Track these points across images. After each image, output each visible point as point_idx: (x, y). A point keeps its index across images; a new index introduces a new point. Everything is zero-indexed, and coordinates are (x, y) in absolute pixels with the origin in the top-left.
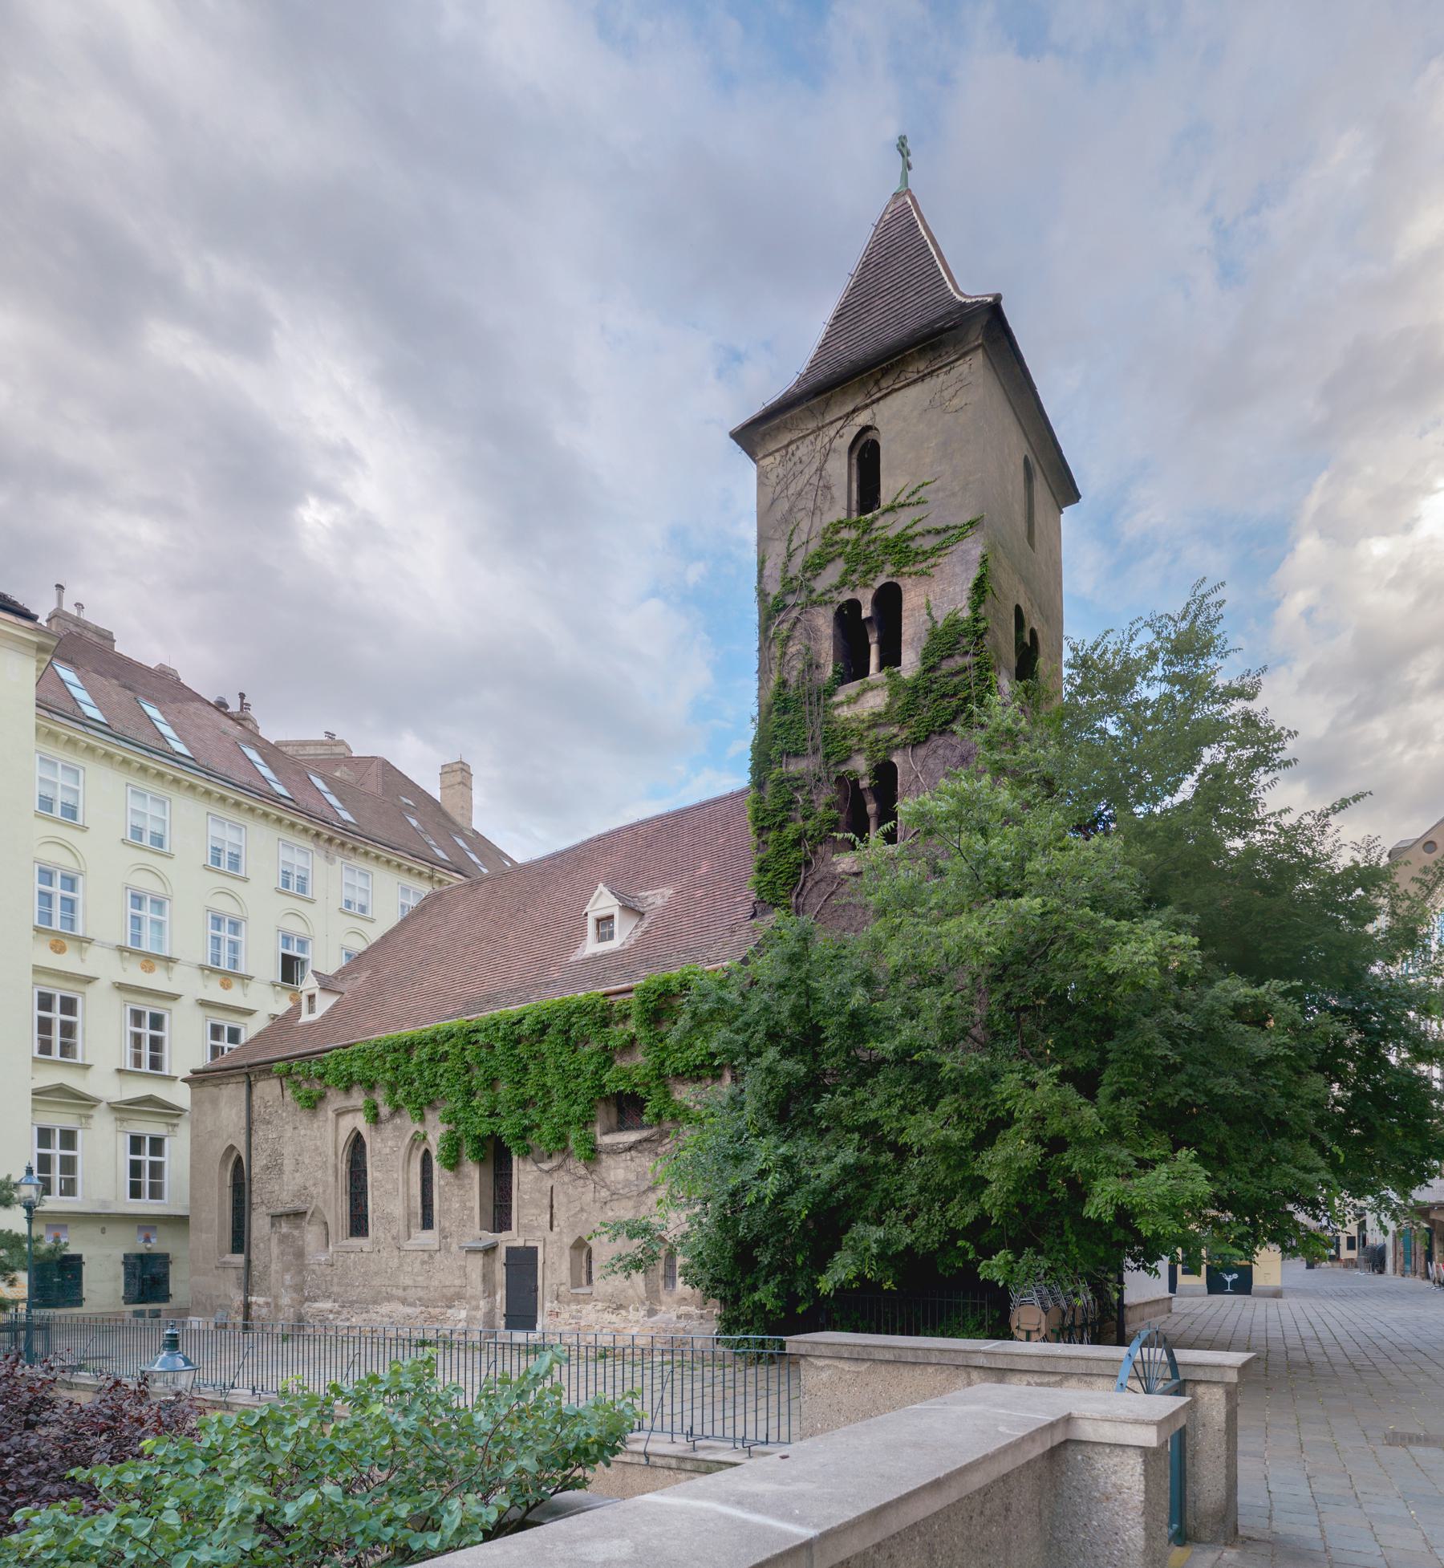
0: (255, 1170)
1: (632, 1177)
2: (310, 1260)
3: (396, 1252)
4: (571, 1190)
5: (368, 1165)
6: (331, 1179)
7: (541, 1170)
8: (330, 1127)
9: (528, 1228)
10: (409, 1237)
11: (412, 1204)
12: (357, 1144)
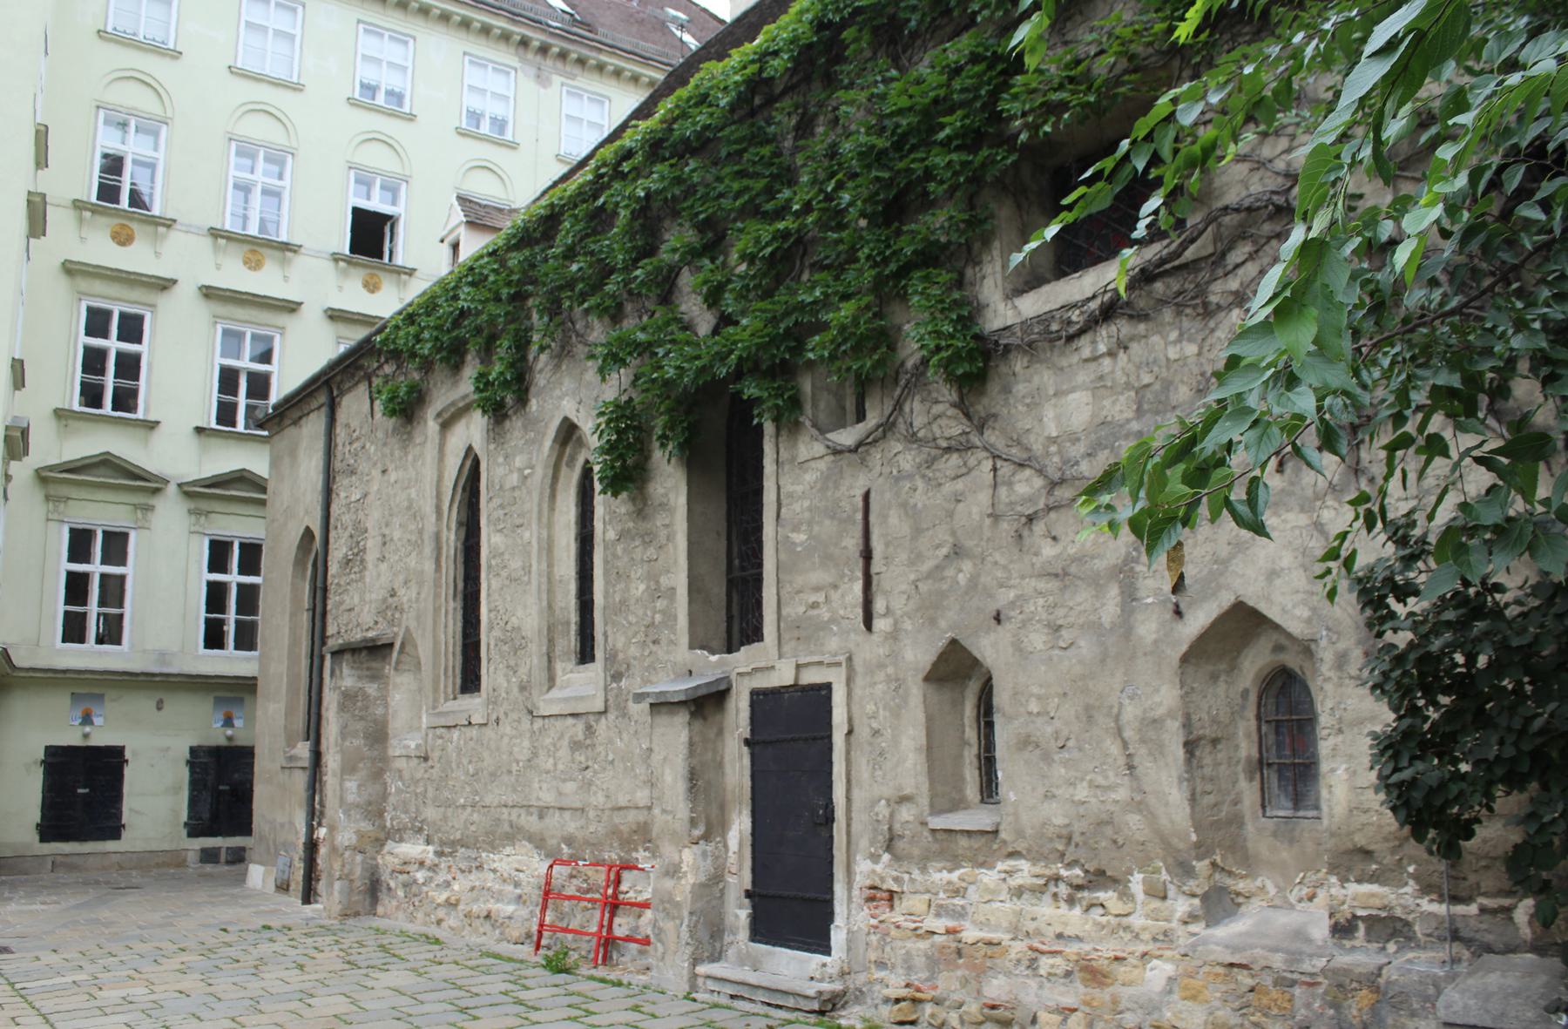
0: (333, 568)
1: (1119, 408)
2: (395, 749)
3: (526, 720)
4: (919, 499)
6: (429, 566)
8: (430, 451)
9: (804, 631)
10: (551, 681)
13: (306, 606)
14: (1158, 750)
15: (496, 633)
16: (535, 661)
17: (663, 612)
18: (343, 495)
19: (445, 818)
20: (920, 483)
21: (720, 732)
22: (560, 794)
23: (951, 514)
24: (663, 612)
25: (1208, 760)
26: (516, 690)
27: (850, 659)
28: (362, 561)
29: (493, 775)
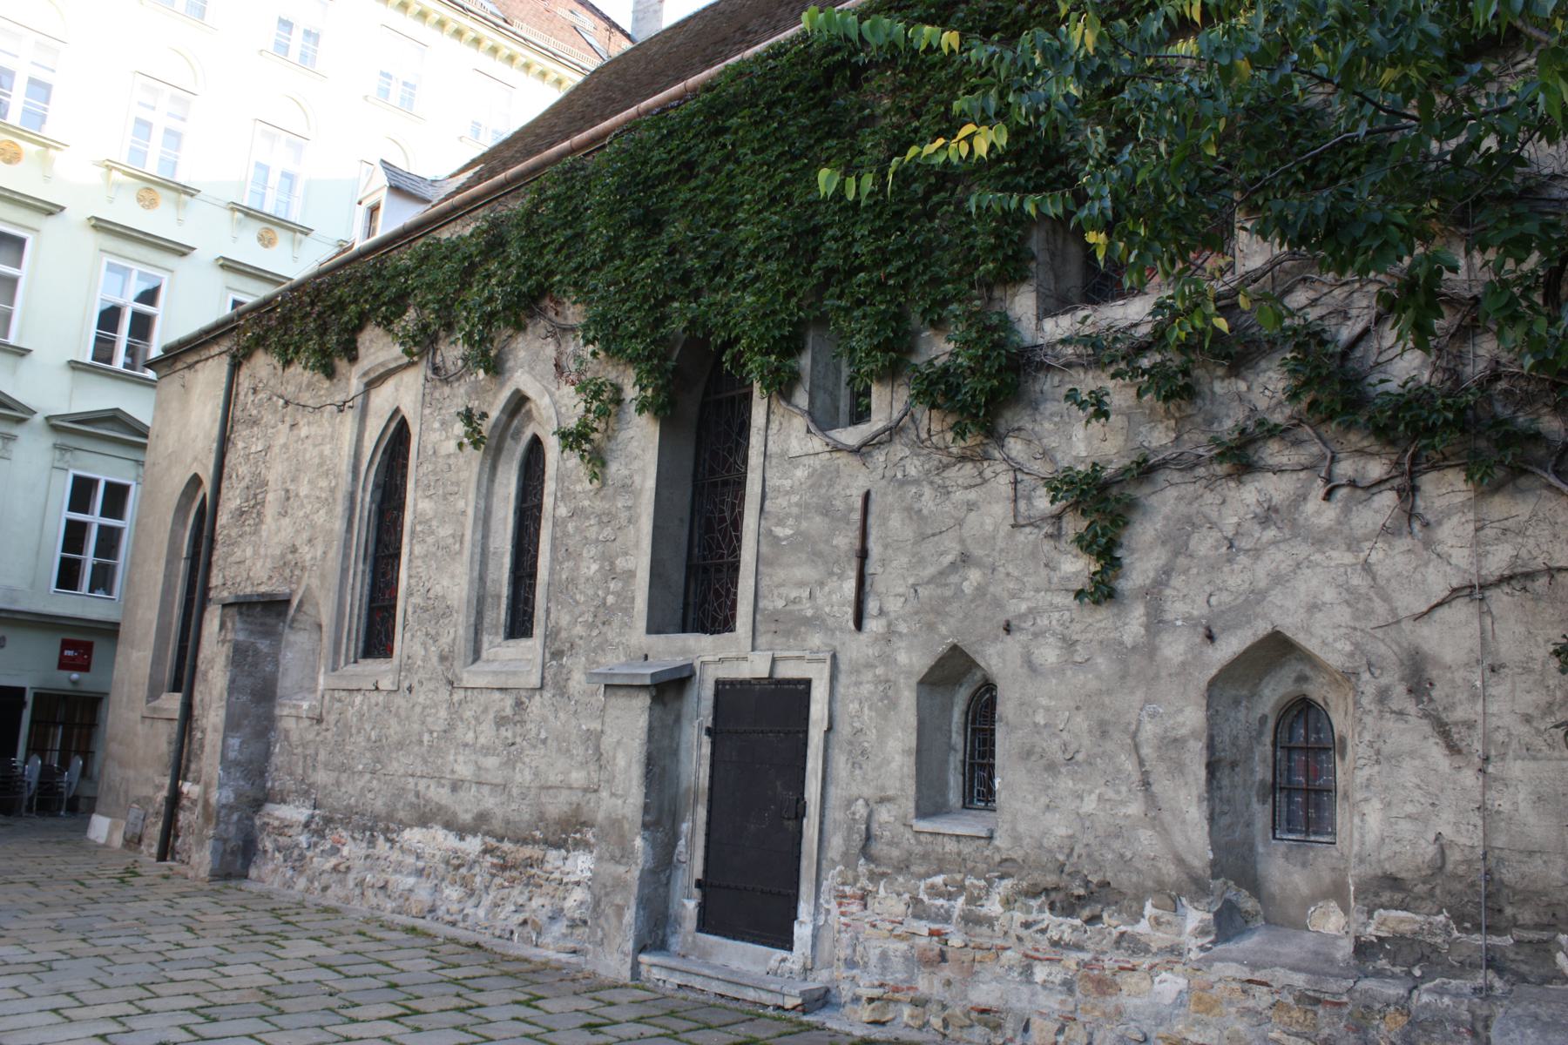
0: (223, 519)
3: (444, 693)
5: (410, 485)
6: (339, 525)
7: (837, 448)
10: (476, 655)
11: (492, 575)
12: (398, 440)
13: (184, 554)
14: (1178, 769)
15: (416, 600)
16: (461, 631)
17: (617, 594)
18: (240, 445)
19: (338, 784)
20: (927, 491)
21: (678, 719)
22: (479, 768)
23: (960, 523)
24: (617, 594)
25: (1225, 782)
26: (435, 660)
27: (834, 657)
28: (259, 514)
29: (400, 745)
